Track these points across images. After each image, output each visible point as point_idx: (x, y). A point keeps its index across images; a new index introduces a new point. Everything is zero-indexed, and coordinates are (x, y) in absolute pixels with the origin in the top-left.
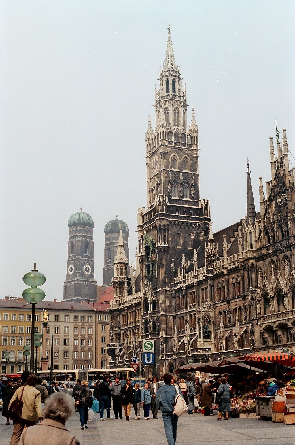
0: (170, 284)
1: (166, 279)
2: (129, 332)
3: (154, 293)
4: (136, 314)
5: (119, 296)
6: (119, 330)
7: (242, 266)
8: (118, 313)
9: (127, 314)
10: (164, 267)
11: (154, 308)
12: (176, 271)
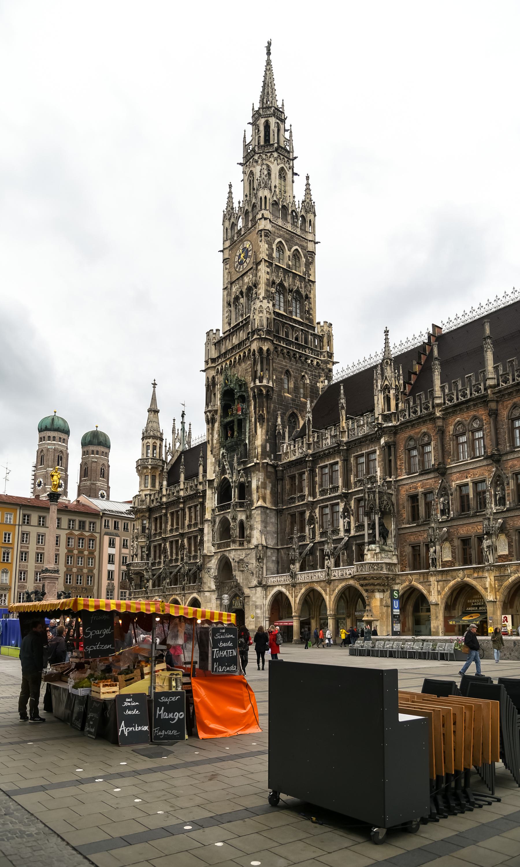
0: (272, 455)
1: (268, 445)
2: (168, 544)
3: (243, 469)
4: (184, 515)
5: (149, 488)
6: (148, 542)
7: (494, 393)
8: (147, 515)
9: (166, 515)
10: (265, 424)
11: (242, 496)
12: (284, 433)
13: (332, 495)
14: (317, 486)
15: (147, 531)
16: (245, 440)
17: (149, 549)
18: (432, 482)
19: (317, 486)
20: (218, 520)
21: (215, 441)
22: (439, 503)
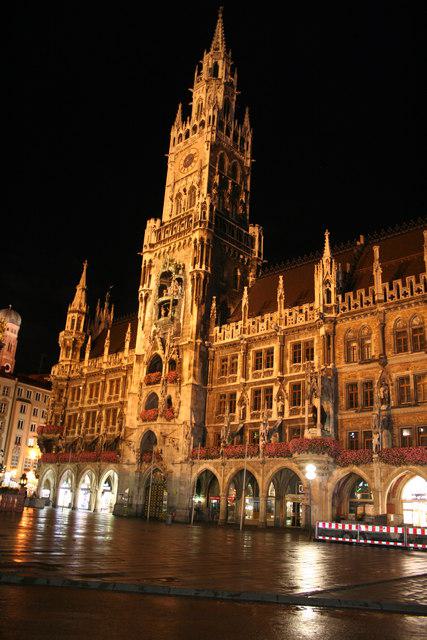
13: (266, 378)
14: (250, 369)
15: (63, 400)
16: (178, 320)
17: (63, 419)
18: (374, 371)
19: (250, 369)
20: (145, 393)
21: (146, 319)
22: (379, 393)
